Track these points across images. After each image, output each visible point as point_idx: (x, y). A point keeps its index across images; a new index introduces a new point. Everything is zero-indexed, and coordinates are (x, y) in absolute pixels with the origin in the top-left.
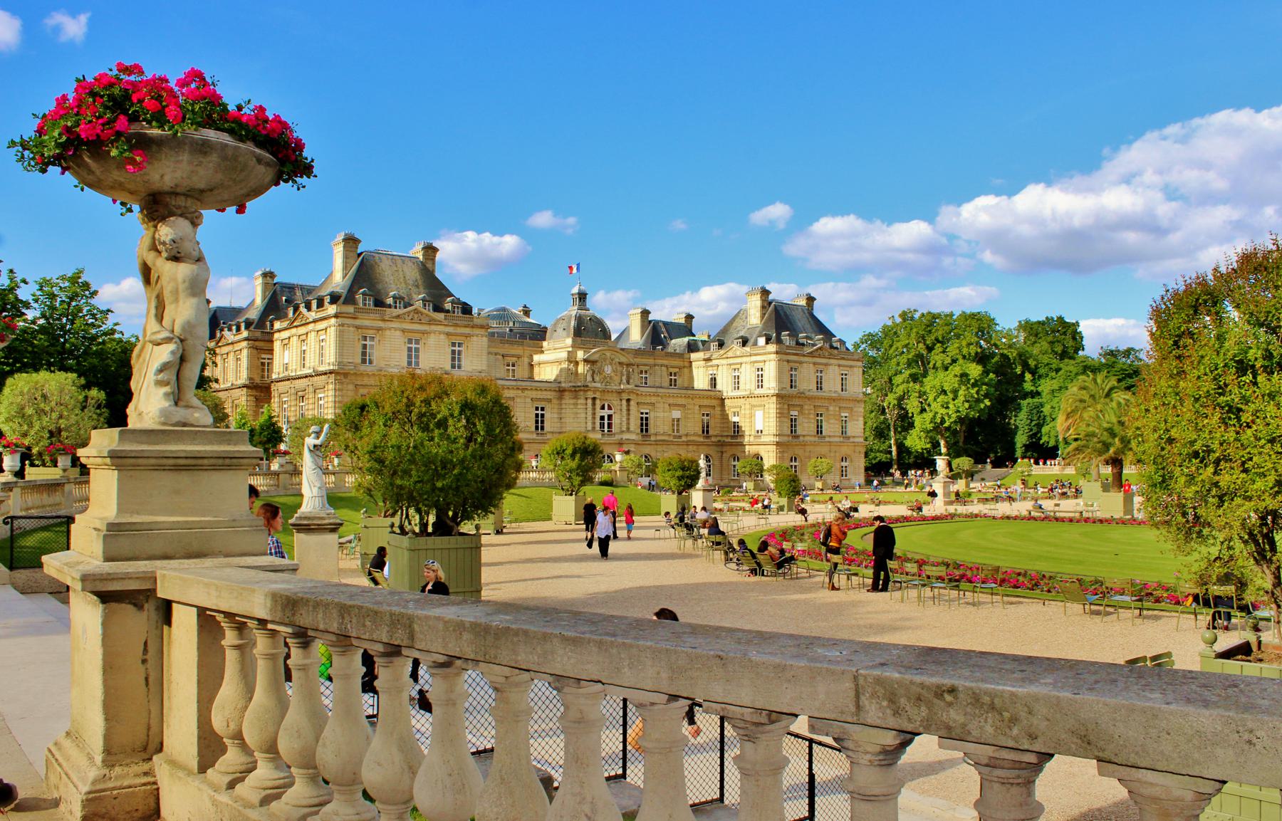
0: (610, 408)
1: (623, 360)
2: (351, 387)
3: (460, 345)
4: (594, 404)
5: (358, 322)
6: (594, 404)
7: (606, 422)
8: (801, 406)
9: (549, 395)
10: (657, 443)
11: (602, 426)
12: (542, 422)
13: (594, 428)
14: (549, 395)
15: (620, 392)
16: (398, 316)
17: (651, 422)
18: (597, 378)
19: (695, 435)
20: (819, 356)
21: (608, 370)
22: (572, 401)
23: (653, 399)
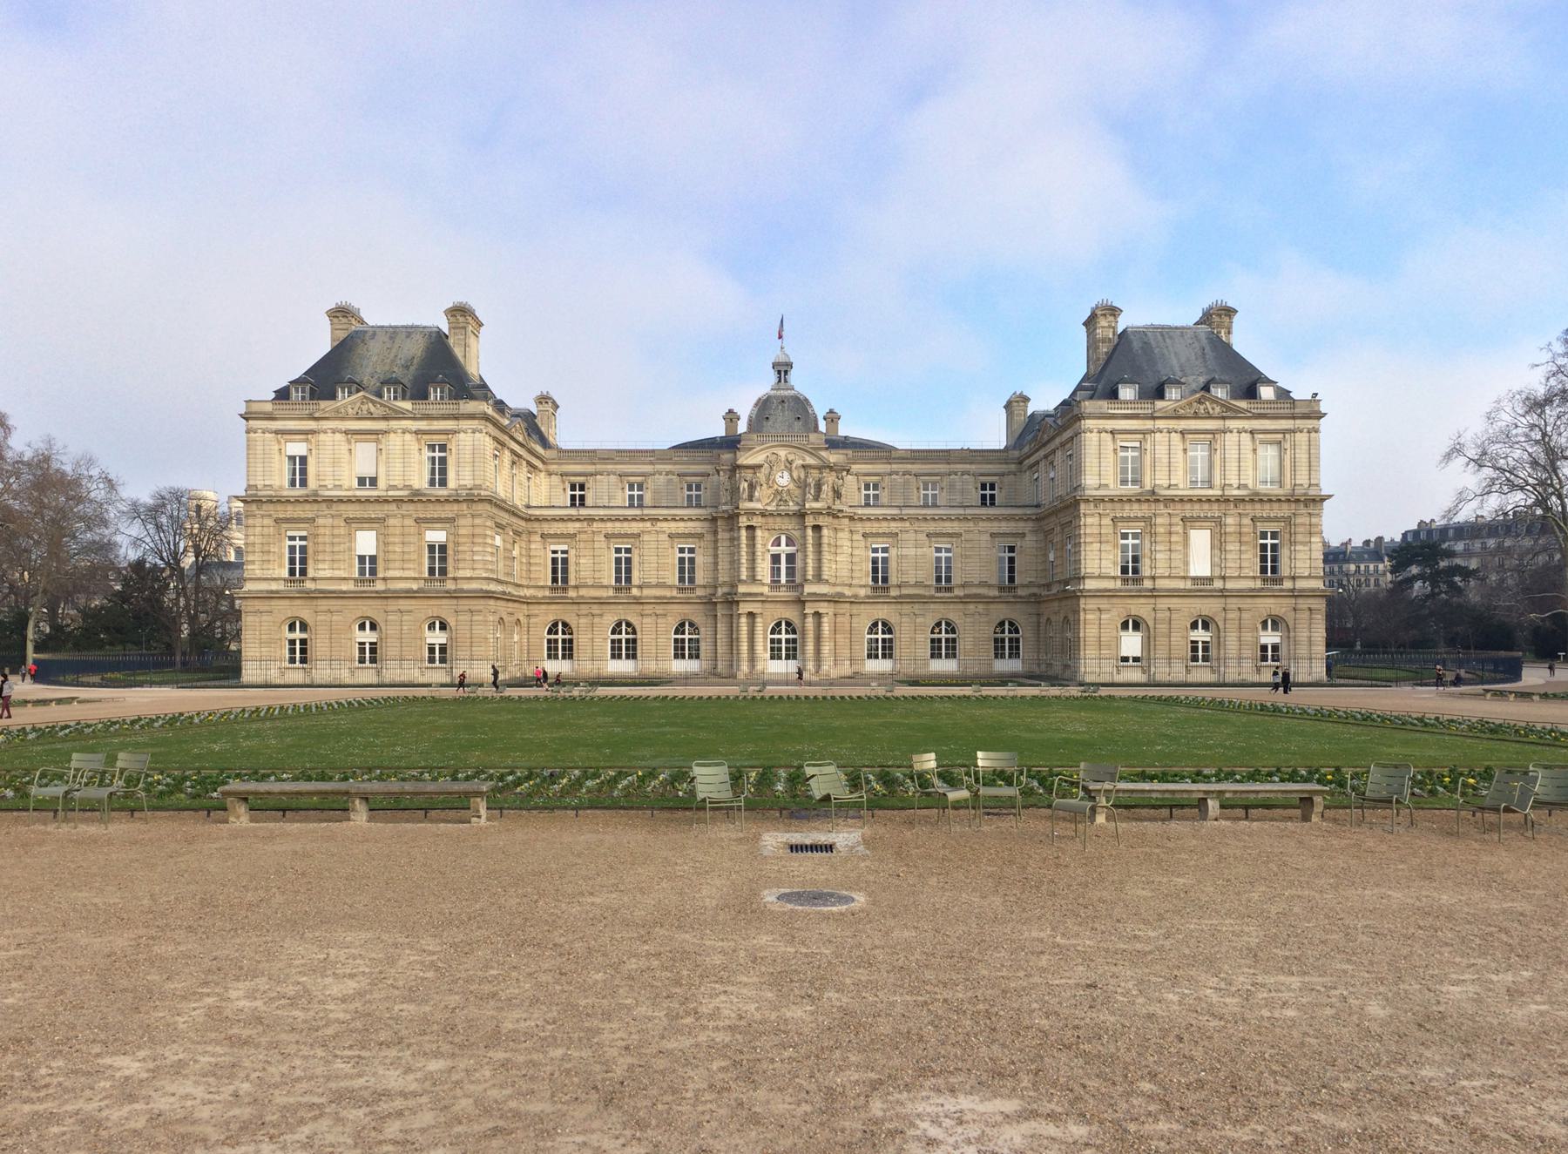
0: (790, 542)
2: (267, 521)
4: (752, 539)
10: (900, 600)
11: (776, 572)
17: (893, 565)
19: (983, 584)
22: (727, 535)
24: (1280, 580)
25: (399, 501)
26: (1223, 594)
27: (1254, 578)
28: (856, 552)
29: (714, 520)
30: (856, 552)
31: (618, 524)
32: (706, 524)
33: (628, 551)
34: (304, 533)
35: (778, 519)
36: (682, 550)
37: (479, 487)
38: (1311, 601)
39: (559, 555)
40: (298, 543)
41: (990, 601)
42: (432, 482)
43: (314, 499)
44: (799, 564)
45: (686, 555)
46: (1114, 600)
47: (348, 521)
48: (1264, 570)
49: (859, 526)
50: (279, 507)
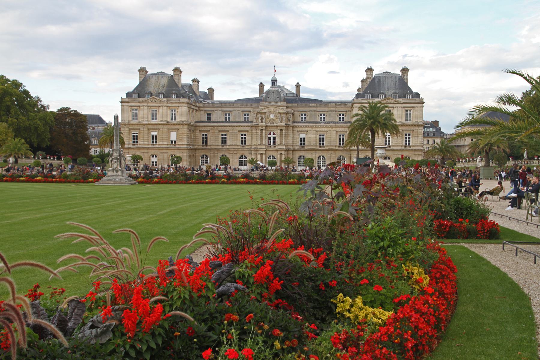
0: (274, 134)
1: (281, 111)
2: (127, 129)
3: (175, 111)
4: (262, 133)
5: (130, 104)
6: (262, 133)
7: (272, 140)
9: (247, 129)
10: (308, 150)
12: (245, 141)
13: (261, 144)
14: (247, 129)
15: (277, 126)
18: (264, 121)
21: (272, 116)
23: (307, 129)
24: (410, 146)
25: (163, 125)
26: (393, 150)
27: (402, 146)
29: (252, 127)
33: (226, 135)
36: (242, 135)
40: (135, 135)
42: (172, 119)
43: (140, 124)
44: (276, 140)
45: (243, 136)
47: (149, 129)
48: (406, 144)
49: (296, 129)
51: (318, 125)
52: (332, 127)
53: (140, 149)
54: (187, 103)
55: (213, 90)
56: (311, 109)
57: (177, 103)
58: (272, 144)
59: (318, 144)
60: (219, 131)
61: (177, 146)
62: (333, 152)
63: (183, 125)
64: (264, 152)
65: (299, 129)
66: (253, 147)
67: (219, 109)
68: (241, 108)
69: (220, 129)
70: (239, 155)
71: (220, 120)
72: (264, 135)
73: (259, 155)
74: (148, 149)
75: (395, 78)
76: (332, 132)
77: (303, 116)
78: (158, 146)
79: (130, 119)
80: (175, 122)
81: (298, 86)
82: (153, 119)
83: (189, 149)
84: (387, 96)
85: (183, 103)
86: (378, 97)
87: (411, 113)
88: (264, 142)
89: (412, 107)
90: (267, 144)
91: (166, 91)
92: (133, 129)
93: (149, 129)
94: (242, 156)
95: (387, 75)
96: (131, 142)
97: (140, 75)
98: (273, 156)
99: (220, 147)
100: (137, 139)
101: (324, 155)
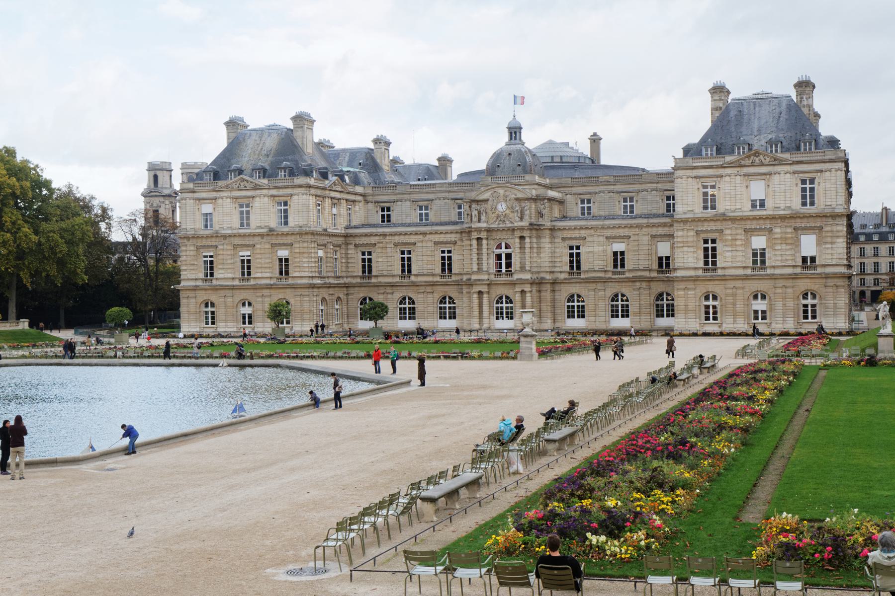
1: (520, 195)
2: (192, 248)
4: (479, 244)
5: (197, 195)
6: (479, 244)
7: (504, 261)
8: (721, 231)
9: (452, 238)
10: (587, 281)
12: (450, 264)
13: (480, 270)
15: (513, 230)
16: (227, 186)
18: (483, 218)
20: (753, 165)
22: (468, 242)
24: (815, 268)
25: (262, 235)
26: (773, 277)
27: (794, 267)
28: (557, 250)
29: (461, 233)
30: (557, 250)
31: (402, 237)
32: (458, 235)
34: (211, 254)
35: (499, 233)
36: (443, 252)
37: (306, 226)
38: (836, 280)
39: (366, 257)
40: (209, 259)
41: (651, 280)
44: (513, 261)
45: (446, 255)
46: (698, 283)
47: (235, 247)
49: (560, 234)
50: (199, 240)
51: (607, 222)
52: (639, 226)
53: (216, 289)
54: (309, 186)
55: (451, 161)
56: (602, 188)
57: (287, 187)
58: (504, 269)
59: (610, 267)
60: (396, 245)
61: (290, 281)
62: (644, 285)
63: (300, 234)
64: (484, 289)
65: (566, 234)
66: (465, 278)
67: (406, 196)
68: (449, 192)
69: (397, 239)
70: (437, 296)
71: (408, 221)
72: (484, 251)
73: (475, 296)
74: (233, 288)
75: (779, 104)
76: (641, 238)
77: (586, 205)
78: (252, 282)
79: (200, 225)
80: (285, 229)
81: (595, 140)
82: (242, 225)
83: (313, 287)
84: (755, 148)
85: (300, 186)
86: (732, 152)
87: (815, 185)
88: (485, 266)
89: (817, 171)
90: (493, 270)
91: (272, 164)
92: (203, 247)
93: (235, 247)
94: (444, 298)
95: (758, 101)
96: (202, 276)
97: (228, 133)
98: (507, 297)
99: (398, 279)
100: (212, 269)
101: (624, 291)
